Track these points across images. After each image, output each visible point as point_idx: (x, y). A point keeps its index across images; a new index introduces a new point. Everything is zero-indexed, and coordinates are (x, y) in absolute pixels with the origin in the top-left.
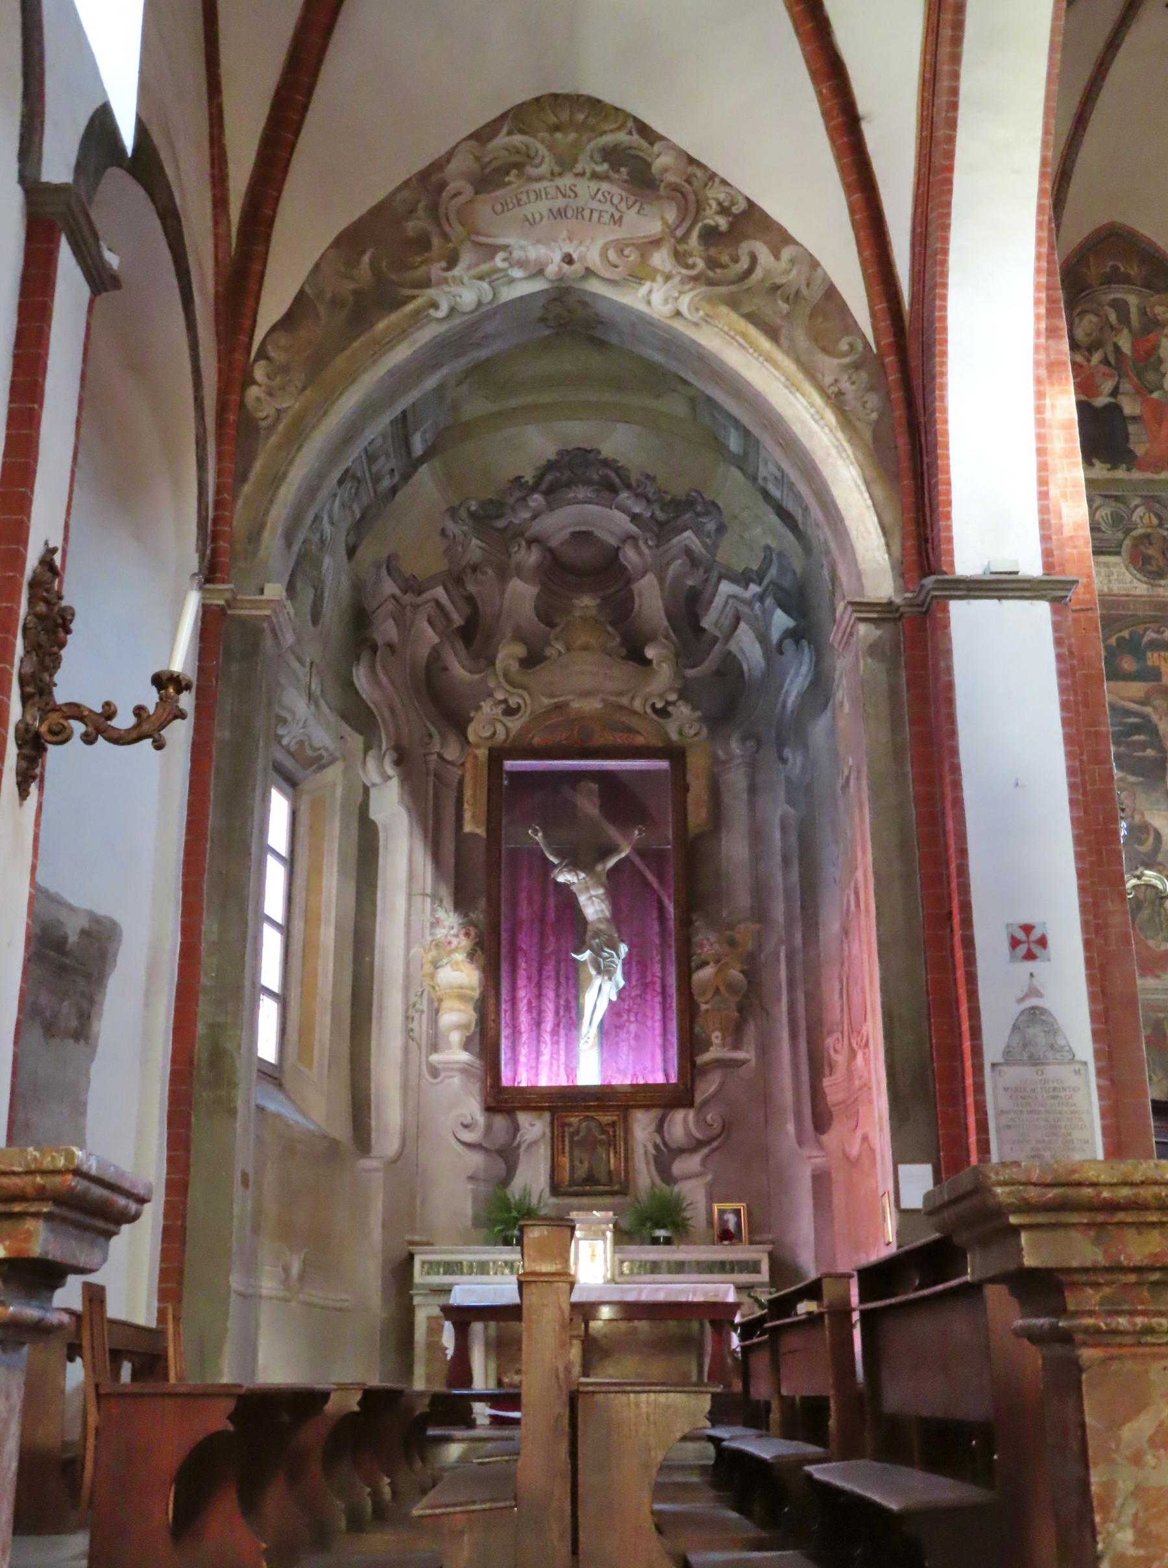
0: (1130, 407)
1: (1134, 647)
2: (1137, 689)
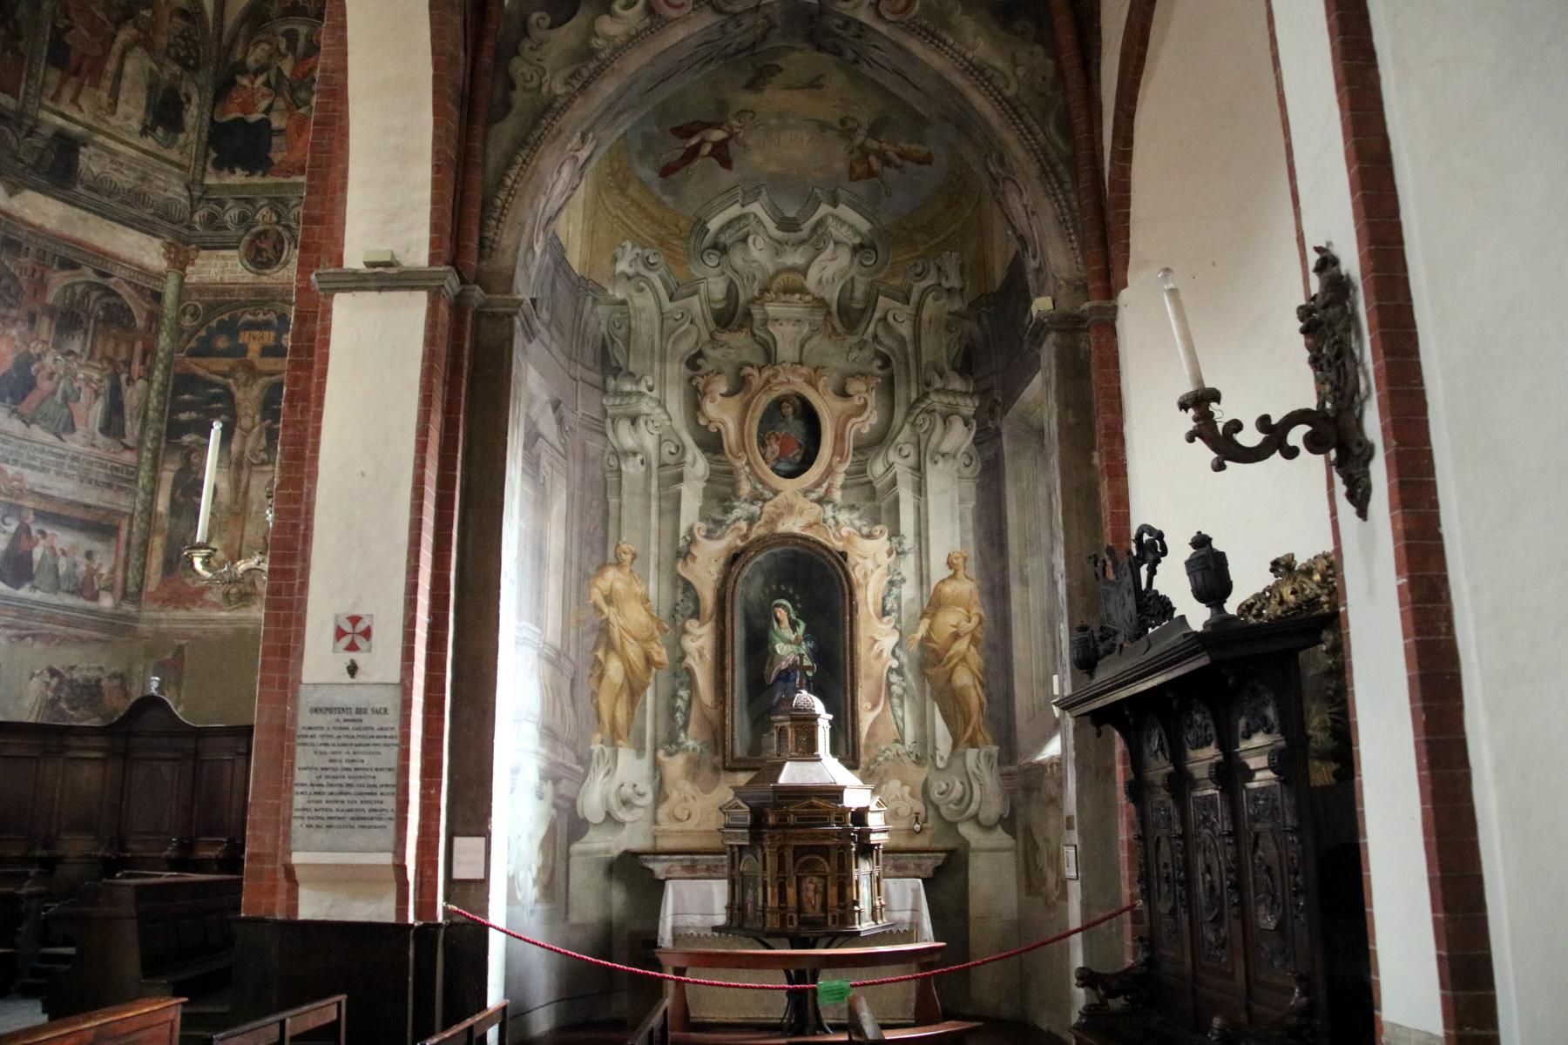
0: (277, 122)
1: (230, 329)
2: (223, 364)
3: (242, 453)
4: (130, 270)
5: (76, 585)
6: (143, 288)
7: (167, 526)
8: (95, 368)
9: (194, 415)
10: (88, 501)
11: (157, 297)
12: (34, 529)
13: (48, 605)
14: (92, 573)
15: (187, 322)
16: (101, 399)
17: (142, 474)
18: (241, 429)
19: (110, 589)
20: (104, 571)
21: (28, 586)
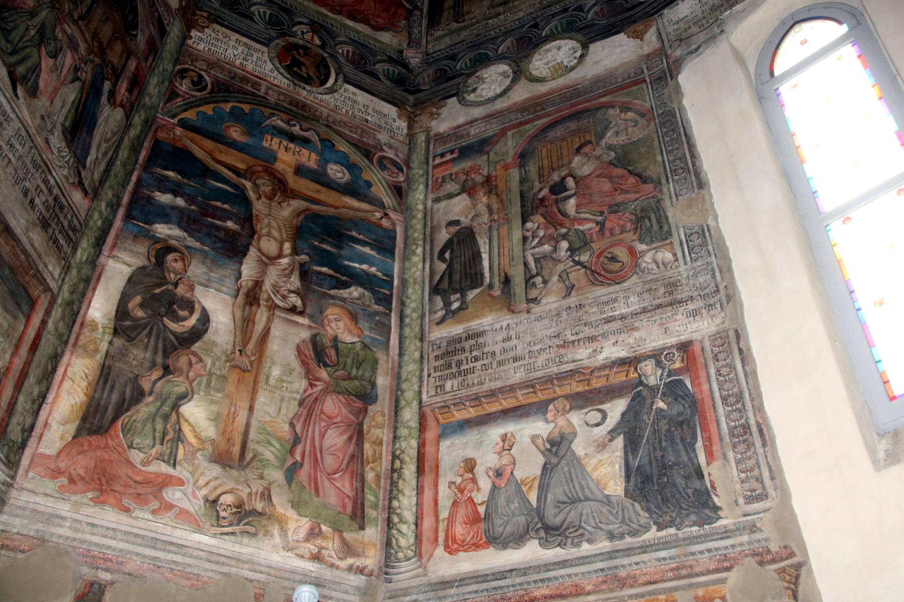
2: (239, 161)
3: (258, 284)
7: (104, 347)
10: (13, 224)
11: (163, 32)
15: (184, 86)
16: (78, 84)
18: (260, 250)
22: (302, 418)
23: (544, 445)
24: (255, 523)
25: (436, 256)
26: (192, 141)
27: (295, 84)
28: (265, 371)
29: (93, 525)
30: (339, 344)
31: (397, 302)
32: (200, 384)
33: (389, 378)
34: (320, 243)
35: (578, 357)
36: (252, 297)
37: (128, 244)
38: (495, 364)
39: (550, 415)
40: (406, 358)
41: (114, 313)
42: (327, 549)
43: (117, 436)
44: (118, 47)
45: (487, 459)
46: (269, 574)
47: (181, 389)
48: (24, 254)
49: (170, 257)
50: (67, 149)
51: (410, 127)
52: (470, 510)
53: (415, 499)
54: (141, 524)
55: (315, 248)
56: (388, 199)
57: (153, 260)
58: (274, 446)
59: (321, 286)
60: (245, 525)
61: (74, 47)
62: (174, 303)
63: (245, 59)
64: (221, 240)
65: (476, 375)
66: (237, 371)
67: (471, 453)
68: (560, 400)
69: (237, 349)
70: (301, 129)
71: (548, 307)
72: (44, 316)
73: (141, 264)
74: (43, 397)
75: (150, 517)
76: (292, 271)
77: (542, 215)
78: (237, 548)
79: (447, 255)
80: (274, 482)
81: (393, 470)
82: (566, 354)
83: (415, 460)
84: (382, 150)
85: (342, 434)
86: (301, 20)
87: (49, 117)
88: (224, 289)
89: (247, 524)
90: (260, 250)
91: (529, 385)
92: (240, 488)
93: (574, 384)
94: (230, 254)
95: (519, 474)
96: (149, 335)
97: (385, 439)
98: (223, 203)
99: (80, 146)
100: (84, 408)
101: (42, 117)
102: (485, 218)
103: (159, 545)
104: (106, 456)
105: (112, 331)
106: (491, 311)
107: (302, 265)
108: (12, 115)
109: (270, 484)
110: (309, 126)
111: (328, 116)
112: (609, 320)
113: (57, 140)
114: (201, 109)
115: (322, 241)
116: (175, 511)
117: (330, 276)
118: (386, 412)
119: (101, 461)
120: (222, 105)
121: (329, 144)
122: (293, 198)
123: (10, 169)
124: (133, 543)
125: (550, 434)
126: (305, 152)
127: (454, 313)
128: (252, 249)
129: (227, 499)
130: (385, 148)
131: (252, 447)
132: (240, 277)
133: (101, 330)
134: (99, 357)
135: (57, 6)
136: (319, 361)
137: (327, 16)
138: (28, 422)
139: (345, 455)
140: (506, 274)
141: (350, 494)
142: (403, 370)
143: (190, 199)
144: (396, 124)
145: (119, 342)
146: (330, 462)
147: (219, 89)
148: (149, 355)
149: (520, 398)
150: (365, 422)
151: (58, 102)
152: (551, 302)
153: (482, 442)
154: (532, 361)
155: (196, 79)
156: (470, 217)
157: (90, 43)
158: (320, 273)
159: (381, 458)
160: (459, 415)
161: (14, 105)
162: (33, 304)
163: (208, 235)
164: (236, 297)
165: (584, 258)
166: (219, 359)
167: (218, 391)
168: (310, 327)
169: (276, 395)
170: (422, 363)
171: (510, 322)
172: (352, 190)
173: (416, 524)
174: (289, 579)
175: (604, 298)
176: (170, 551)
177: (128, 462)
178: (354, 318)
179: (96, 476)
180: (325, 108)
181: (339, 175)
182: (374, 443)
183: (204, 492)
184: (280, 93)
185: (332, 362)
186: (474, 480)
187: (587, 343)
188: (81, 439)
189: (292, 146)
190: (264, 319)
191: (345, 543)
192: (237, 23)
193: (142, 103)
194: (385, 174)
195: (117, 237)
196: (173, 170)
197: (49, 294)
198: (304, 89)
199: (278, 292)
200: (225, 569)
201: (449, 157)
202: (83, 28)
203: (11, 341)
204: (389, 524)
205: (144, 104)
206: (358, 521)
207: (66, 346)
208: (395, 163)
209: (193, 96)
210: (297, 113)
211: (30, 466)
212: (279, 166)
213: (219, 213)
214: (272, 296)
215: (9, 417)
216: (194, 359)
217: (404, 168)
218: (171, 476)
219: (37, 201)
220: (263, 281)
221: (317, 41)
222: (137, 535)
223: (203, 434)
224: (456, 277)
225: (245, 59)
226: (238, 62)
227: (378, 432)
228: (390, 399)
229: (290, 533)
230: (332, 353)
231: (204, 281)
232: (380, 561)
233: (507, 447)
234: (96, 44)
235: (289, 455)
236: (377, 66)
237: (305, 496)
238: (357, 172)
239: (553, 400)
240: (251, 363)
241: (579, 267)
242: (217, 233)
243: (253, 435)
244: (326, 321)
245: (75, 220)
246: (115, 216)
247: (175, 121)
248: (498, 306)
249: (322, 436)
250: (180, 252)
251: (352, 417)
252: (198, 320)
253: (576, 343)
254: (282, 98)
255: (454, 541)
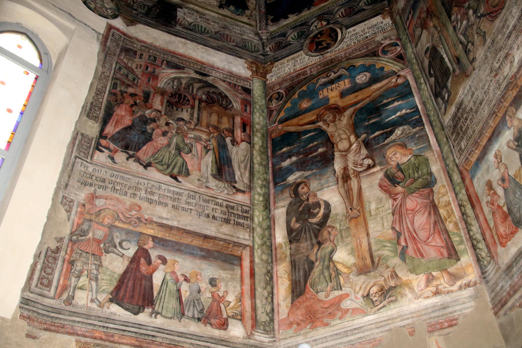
2: (311, 116)
3: (345, 169)
4: (224, 74)
5: (201, 311)
6: (235, 85)
7: (288, 252)
8: (204, 132)
9: (294, 159)
10: (208, 233)
11: (248, 91)
12: (154, 254)
13: (170, 333)
14: (217, 300)
15: (274, 104)
16: (210, 153)
17: (257, 213)
18: (340, 151)
19: (240, 317)
20: (231, 298)
21: (148, 310)
22: (397, 221)
23: (514, 144)
24: (394, 294)
25: (428, 76)
26: (288, 126)
27: (322, 55)
28: (367, 210)
29: (315, 340)
30: (402, 167)
31: (425, 117)
32: (338, 240)
33: (439, 163)
34: (368, 122)
35: (505, 74)
36: (346, 178)
37: (280, 197)
38: (474, 114)
39: (509, 124)
40: (442, 145)
41: (286, 233)
42: (441, 284)
43: (310, 291)
44: (225, 120)
45: (495, 175)
46: (413, 317)
47: (330, 248)
48: (221, 241)
49: (300, 189)
50: (220, 183)
51: (392, 18)
52: (501, 213)
53: (477, 224)
54: (337, 327)
55: (367, 126)
56: (395, 67)
57: (293, 196)
58: (388, 246)
59: (378, 143)
60: (388, 298)
61: (198, 139)
62: (310, 209)
63: (294, 66)
64: (319, 161)
65: (470, 129)
66: (353, 220)
67: (487, 178)
68: (509, 109)
69: (349, 209)
70: (335, 73)
71: (480, 57)
72: (250, 259)
73: (288, 202)
74: (272, 293)
75: (339, 322)
76: (360, 147)
77: (456, 6)
78: (389, 313)
79: (432, 72)
80: (395, 266)
81: (463, 214)
82: (500, 78)
83: (468, 201)
84: (382, 44)
85: (423, 214)
86: (312, 21)
87: (202, 177)
88: (331, 184)
89: (390, 296)
90: (340, 151)
91: (493, 114)
92: (378, 280)
93: (511, 93)
94: (326, 165)
95: (512, 173)
96: (305, 233)
97: (451, 199)
98: (313, 143)
99: (227, 176)
100: (291, 287)
101: (199, 180)
102: (436, 35)
103: (349, 333)
104: (308, 303)
105: (289, 243)
106: (460, 85)
107: (363, 141)
108: (181, 191)
109: (394, 268)
110: (338, 68)
111: (345, 54)
112: (509, 37)
113: (213, 183)
114: (285, 107)
115: (370, 119)
116: (350, 311)
117: (381, 134)
118: (445, 183)
119: (307, 308)
120: (294, 97)
121: (352, 68)
122: (345, 111)
123: (194, 212)
124: (336, 339)
125: (514, 135)
126: (342, 83)
127: (447, 101)
128: (336, 153)
129: (375, 289)
130: (383, 42)
131: (376, 254)
132: (335, 172)
133: (284, 245)
134: (288, 259)
135: (180, 131)
136: (394, 184)
137: (324, 6)
138: (268, 309)
139: (430, 225)
140: (456, 57)
141: (443, 245)
142: (444, 153)
143: (298, 154)
144: (384, 23)
145: (293, 246)
146: (422, 235)
147: (289, 91)
148: (309, 243)
149: (492, 124)
150: (434, 198)
151: (203, 168)
152: (480, 53)
153: (488, 166)
154: (487, 97)
155: (277, 96)
156: (431, 41)
157: (208, 131)
158: (375, 137)
159: (453, 212)
160: (473, 159)
161: (180, 187)
162: (240, 259)
163: (312, 164)
164: (338, 183)
165: (482, 11)
166: (342, 221)
167: (347, 237)
168: (381, 169)
169: (378, 218)
170: (448, 142)
171: (470, 83)
172: (374, 80)
173: (484, 239)
174: (425, 314)
175: (501, 25)
176: (356, 334)
177: (320, 301)
178: (404, 146)
179: (308, 316)
180: (342, 51)
181: (363, 79)
182: (445, 206)
183: (361, 293)
184: (317, 67)
185: (402, 179)
186: (495, 193)
187: (506, 62)
188: (295, 303)
189: (334, 86)
190: (356, 183)
191: (451, 275)
192: (284, 53)
193: (255, 130)
194: (390, 55)
195: (274, 198)
196: (285, 147)
197: (248, 249)
198: (328, 52)
199: (357, 165)
200: (387, 328)
201: (410, 16)
202: (200, 128)
203: (237, 281)
204: (474, 247)
205: (257, 130)
206: (454, 257)
207: (273, 264)
208: (391, 45)
209: (279, 105)
210: (329, 67)
211: (279, 328)
212: (332, 101)
213: (313, 149)
214: (355, 169)
215: (255, 313)
216: (330, 229)
217: (398, 42)
218: (342, 295)
219: (216, 215)
220: (347, 165)
221: (324, 23)
222: (337, 334)
223: (349, 264)
224: (440, 80)
225: (294, 66)
226: (292, 71)
227: (445, 198)
228: (445, 175)
229: (415, 288)
230: (400, 174)
231: (320, 188)
232: (478, 273)
233: (499, 160)
234: (211, 128)
235: (398, 246)
236: (360, 5)
237: (416, 262)
238: (372, 69)
239: (506, 111)
240: (359, 211)
241: (482, 18)
242: (316, 160)
243: (374, 248)
244: (389, 160)
245: (244, 208)
246: (269, 189)
247: (277, 123)
248: (461, 79)
249: (412, 223)
250: (303, 182)
251: (426, 201)
252: (324, 208)
253: (501, 66)
254: (319, 67)
255: (502, 237)
